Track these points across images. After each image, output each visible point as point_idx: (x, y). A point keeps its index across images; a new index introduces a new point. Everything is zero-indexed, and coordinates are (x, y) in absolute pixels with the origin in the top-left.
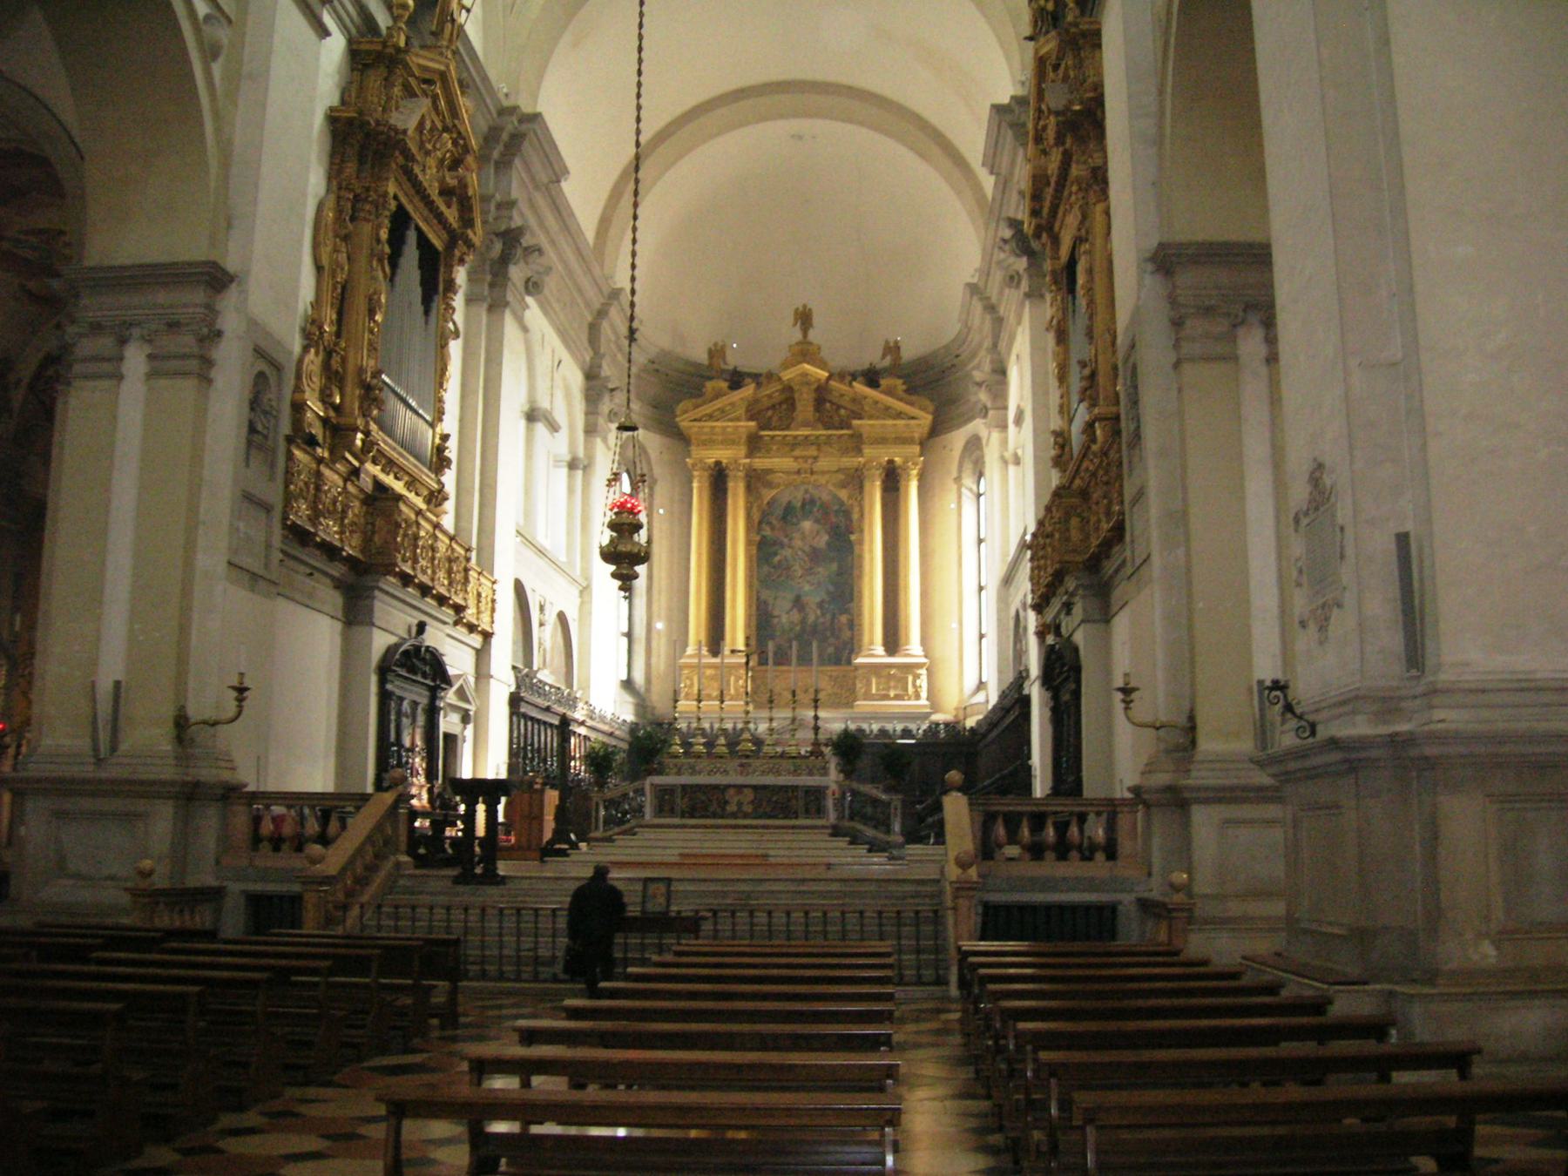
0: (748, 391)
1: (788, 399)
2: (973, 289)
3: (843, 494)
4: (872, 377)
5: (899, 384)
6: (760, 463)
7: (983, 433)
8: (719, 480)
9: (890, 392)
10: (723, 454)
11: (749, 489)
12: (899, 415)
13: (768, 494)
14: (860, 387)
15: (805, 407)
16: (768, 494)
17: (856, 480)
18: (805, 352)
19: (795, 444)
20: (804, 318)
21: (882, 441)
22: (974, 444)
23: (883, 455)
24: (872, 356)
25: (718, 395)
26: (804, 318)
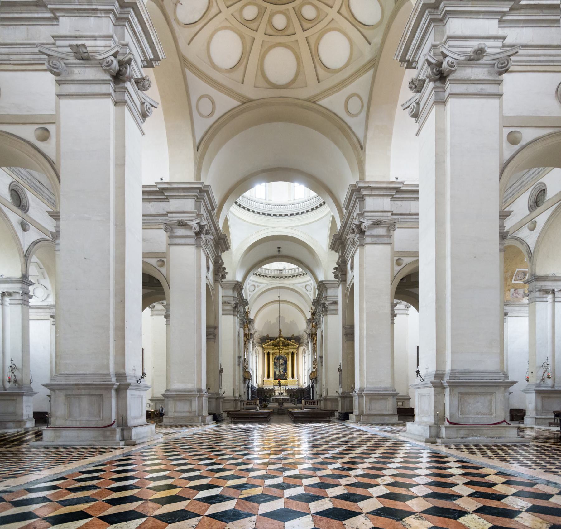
0: (272, 342)
1: (279, 342)
2: (305, 331)
3: (286, 356)
4: (290, 339)
5: (294, 341)
6: (274, 351)
7: (306, 348)
8: (268, 354)
9: (293, 342)
10: (270, 351)
11: (273, 355)
12: (294, 345)
13: (275, 356)
14: (288, 341)
15: (281, 344)
16: (275, 356)
17: (287, 354)
18: (280, 336)
19: (279, 349)
20: (280, 331)
21: (292, 349)
22: (304, 349)
23: (292, 350)
24: (290, 336)
25: (268, 342)
26: (280, 331)
